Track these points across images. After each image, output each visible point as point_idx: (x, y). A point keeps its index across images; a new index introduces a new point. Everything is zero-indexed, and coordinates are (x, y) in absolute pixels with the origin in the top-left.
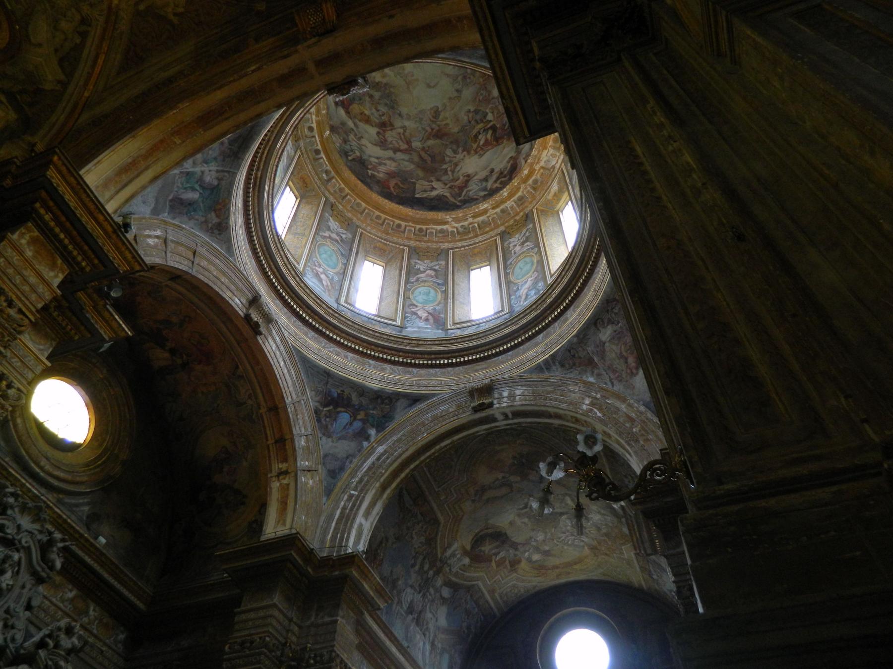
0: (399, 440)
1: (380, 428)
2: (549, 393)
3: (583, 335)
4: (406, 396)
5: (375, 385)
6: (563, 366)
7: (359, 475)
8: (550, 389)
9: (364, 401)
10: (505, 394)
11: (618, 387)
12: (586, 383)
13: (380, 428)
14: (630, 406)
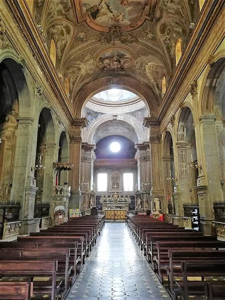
0: (99, 122)
1: (96, 118)
2: (127, 119)
3: (135, 111)
4: (101, 113)
5: (96, 111)
6: (130, 114)
7: (92, 127)
8: (127, 118)
9: (93, 113)
10: (119, 117)
11: (139, 122)
12: (133, 119)
13: (96, 118)
14: (140, 126)
